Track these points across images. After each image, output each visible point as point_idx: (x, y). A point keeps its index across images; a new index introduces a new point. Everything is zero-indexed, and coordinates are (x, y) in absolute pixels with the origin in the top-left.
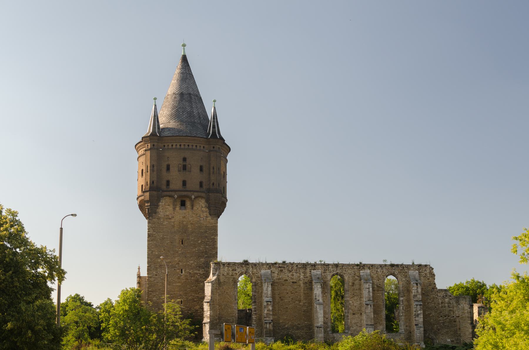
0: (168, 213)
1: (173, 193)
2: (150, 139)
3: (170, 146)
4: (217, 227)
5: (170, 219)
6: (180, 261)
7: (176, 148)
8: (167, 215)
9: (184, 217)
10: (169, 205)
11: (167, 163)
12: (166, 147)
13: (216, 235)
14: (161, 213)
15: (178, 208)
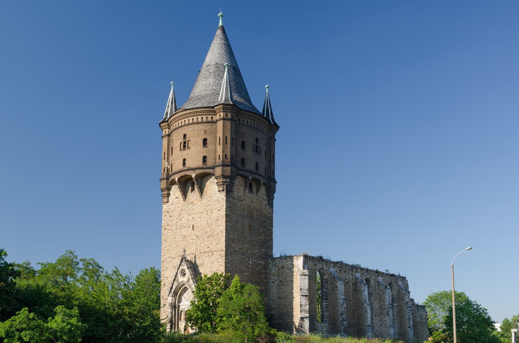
0: (240, 194)
1: (248, 174)
2: (232, 109)
3: (245, 122)
4: (272, 217)
5: (242, 201)
6: (248, 249)
7: (251, 125)
8: (240, 197)
9: (251, 202)
10: (241, 186)
11: (242, 139)
12: (241, 122)
13: (272, 226)
14: (236, 193)
15: (247, 191)
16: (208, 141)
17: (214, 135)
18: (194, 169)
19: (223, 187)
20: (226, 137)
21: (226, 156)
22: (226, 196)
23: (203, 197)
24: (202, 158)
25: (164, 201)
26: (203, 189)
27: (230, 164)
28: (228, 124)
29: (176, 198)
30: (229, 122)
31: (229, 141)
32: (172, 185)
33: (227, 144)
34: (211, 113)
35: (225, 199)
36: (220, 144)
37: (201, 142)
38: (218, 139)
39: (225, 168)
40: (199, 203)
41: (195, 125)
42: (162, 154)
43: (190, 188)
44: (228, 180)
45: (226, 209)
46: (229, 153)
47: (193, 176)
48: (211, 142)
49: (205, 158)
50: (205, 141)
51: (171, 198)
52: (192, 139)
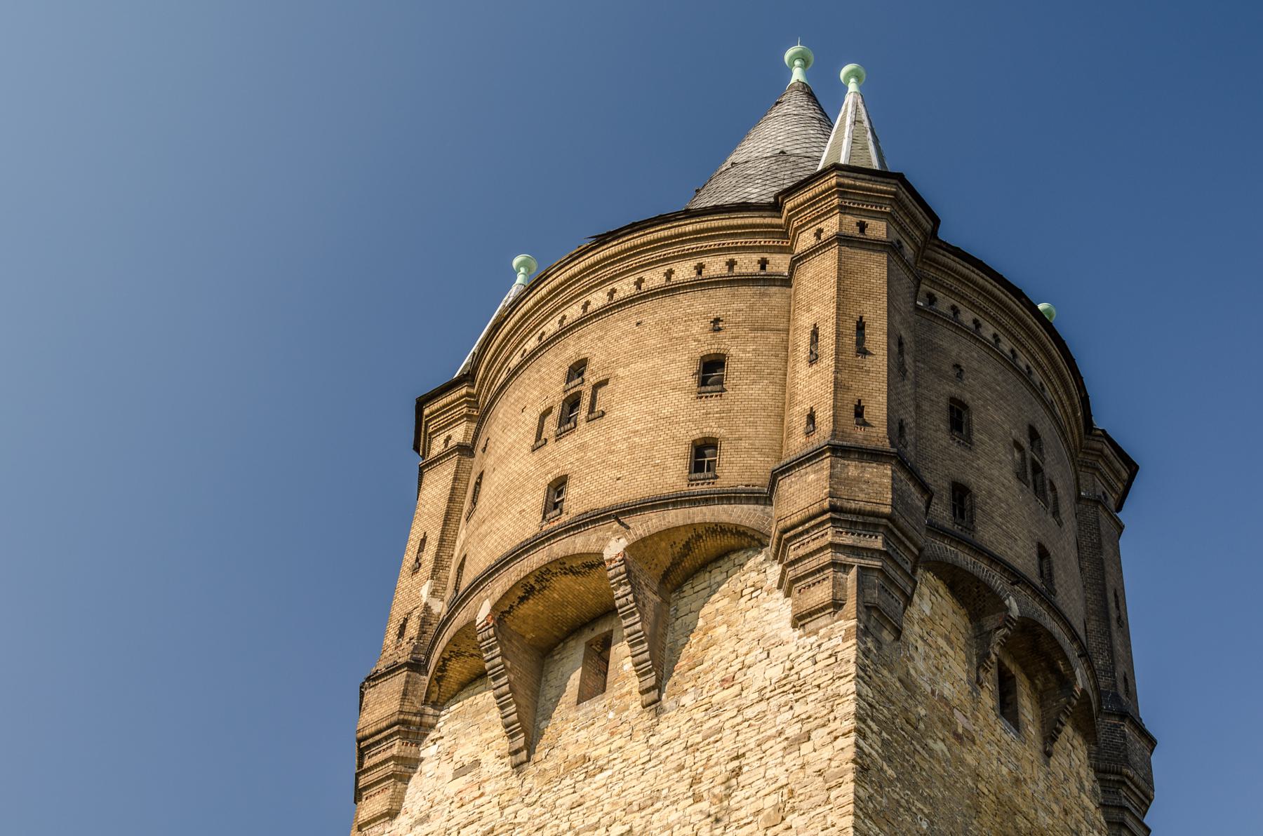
16: (733, 370)
17: (773, 338)
18: (619, 514)
19: (837, 584)
20: (861, 326)
21: (859, 411)
22: (863, 633)
23: (667, 702)
24: (684, 450)
25: (364, 815)
26: (675, 653)
27: (886, 445)
28: (875, 268)
29: (460, 771)
30: (882, 258)
31: (877, 339)
32: (439, 705)
33: (862, 351)
34: (762, 241)
35: (850, 651)
36: (814, 359)
37: (683, 370)
38: (804, 340)
39: (852, 469)
40: (637, 750)
41: (648, 305)
42: (406, 540)
43: (575, 679)
44: (878, 543)
45: (859, 717)
46: (883, 398)
47: (614, 548)
48: (751, 370)
49: (702, 454)
50: (711, 370)
51: (416, 794)
52: (620, 372)
